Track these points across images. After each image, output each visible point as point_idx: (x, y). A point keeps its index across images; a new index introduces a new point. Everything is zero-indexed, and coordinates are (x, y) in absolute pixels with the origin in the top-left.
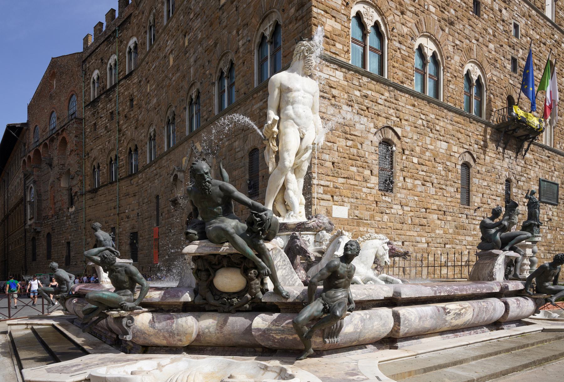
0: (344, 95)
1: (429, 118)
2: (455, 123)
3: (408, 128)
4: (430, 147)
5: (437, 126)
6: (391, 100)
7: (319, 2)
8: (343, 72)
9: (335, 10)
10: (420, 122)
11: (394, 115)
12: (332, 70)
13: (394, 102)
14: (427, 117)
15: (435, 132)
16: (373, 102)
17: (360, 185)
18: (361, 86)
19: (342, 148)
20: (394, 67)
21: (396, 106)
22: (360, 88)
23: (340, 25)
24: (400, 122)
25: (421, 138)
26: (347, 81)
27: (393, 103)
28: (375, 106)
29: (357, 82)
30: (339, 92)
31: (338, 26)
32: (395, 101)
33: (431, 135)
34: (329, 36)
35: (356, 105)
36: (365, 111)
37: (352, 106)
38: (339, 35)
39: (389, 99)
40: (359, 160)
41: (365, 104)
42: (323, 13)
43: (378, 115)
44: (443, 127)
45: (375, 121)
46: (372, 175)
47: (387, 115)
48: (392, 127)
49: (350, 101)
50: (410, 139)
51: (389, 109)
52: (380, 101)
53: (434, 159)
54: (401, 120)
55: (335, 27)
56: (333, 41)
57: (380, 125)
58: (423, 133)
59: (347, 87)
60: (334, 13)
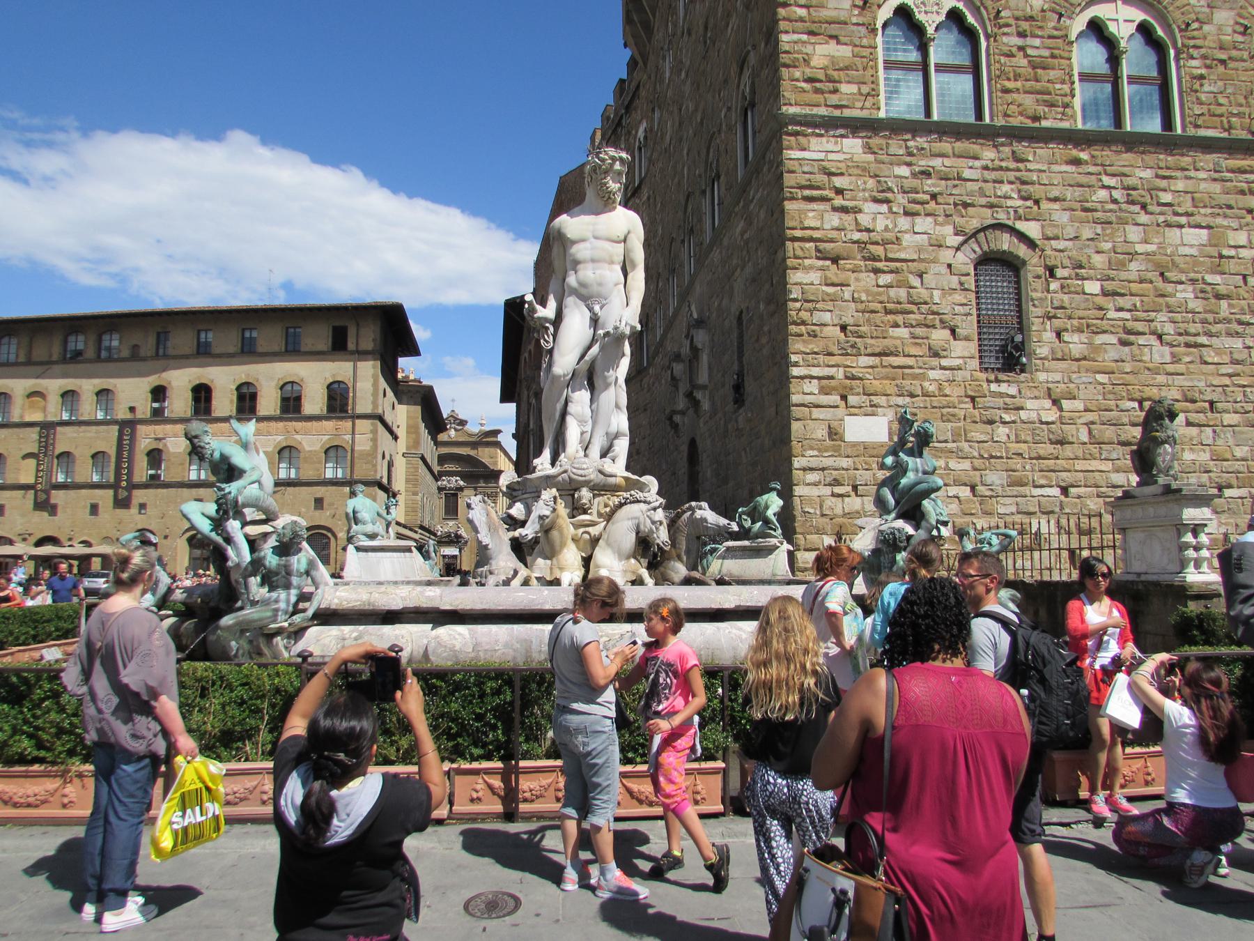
0: (865, 183)
1: (1129, 181)
2: (1229, 175)
3: (1064, 217)
4: (1140, 248)
5: (1161, 194)
6: (1004, 164)
7: (796, 21)
8: (862, 137)
9: (834, 23)
10: (1102, 194)
11: (1016, 196)
12: (833, 140)
13: (1011, 167)
14: (1124, 178)
15: (1158, 209)
16: (950, 179)
17: (921, 364)
18: (910, 154)
19: (868, 292)
20: (1006, 91)
21: (1018, 174)
22: (908, 159)
23: (850, 48)
24: (1036, 208)
25: (1108, 232)
26: (875, 153)
27: (1008, 169)
28: (955, 186)
29: (901, 147)
30: (853, 178)
31: (844, 52)
32: (1012, 165)
33: (1143, 218)
34: (822, 77)
35: (900, 196)
36: (928, 203)
37: (887, 201)
38: (847, 68)
39: (997, 162)
40: (916, 311)
41: (926, 188)
42: (805, 37)
43: (966, 205)
44: (1187, 192)
45: (957, 219)
46: (955, 339)
47: (993, 200)
48: (1010, 223)
49: (883, 191)
50: (1071, 239)
51: (997, 185)
52: (967, 174)
53: (1162, 274)
54: (1037, 202)
55: (837, 54)
56: (831, 85)
57: (975, 224)
58: (1114, 219)
59: (873, 165)
60: (834, 29)
